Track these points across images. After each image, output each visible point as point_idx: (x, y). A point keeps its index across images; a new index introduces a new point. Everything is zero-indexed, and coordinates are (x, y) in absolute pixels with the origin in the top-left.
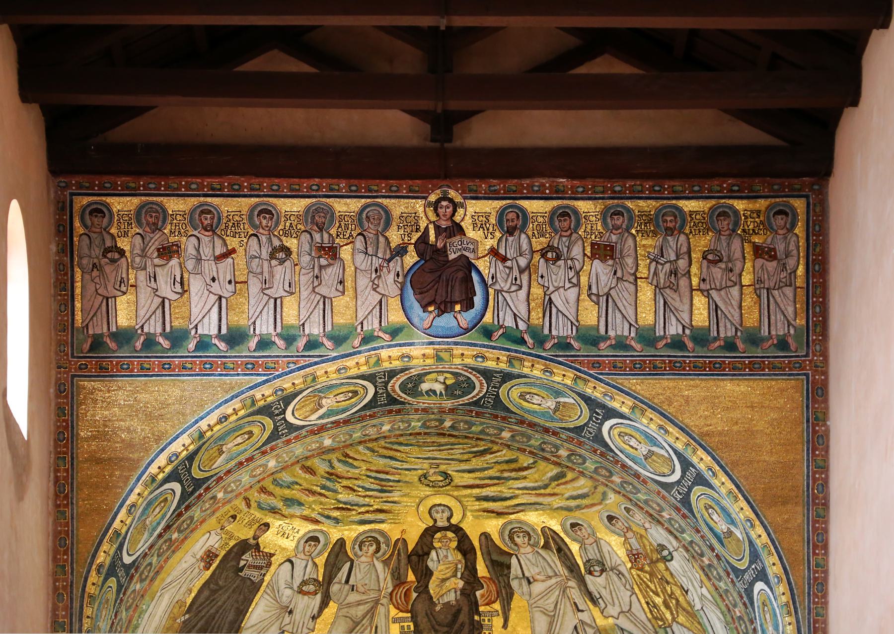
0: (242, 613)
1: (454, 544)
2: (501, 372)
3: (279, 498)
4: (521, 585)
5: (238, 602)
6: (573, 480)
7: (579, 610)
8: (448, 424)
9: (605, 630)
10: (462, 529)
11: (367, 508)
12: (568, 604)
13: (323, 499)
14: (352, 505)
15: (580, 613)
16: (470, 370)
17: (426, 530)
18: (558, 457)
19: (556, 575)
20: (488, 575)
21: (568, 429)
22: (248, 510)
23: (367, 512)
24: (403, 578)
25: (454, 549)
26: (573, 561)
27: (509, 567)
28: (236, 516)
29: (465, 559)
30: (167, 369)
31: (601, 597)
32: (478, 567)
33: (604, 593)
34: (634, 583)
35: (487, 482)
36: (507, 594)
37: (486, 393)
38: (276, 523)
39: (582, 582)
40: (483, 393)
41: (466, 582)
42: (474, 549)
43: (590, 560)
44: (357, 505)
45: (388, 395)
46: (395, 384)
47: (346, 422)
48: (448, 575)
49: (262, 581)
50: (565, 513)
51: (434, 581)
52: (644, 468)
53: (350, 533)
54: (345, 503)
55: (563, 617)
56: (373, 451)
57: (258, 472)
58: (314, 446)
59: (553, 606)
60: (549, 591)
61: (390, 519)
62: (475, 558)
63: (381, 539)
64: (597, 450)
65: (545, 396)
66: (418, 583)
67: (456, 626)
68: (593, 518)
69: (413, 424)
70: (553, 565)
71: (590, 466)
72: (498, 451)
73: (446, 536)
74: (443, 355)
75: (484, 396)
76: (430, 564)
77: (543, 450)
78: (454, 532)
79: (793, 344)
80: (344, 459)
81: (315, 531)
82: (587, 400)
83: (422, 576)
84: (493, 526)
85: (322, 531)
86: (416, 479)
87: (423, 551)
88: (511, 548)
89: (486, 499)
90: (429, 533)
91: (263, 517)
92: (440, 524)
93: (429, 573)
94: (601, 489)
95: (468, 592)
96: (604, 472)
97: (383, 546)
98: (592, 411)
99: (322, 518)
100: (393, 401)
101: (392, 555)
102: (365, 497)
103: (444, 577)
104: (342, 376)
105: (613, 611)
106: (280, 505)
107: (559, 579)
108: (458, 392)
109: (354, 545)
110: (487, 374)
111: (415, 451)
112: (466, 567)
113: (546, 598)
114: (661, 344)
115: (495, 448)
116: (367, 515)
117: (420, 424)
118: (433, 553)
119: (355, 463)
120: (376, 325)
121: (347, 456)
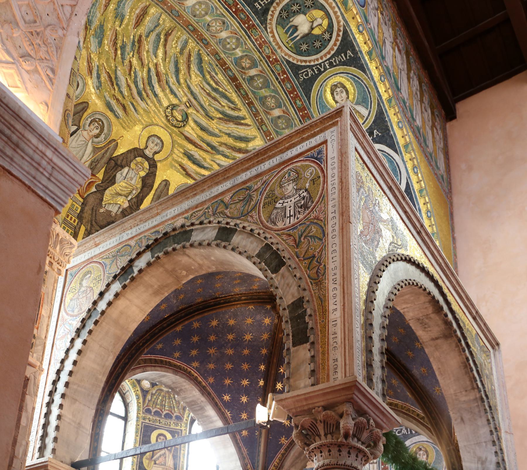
1: (143, 174)
8: (253, 72)
10: (156, 167)
25: (140, 177)
35: (204, 146)
37: (317, 65)
40: (316, 63)
66: (102, 183)
69: (237, 51)
75: (311, 67)
76: (118, 175)
78: (149, 166)
83: (107, 180)
87: (121, 163)
89: (190, 157)
117: (240, 54)
118: (126, 170)
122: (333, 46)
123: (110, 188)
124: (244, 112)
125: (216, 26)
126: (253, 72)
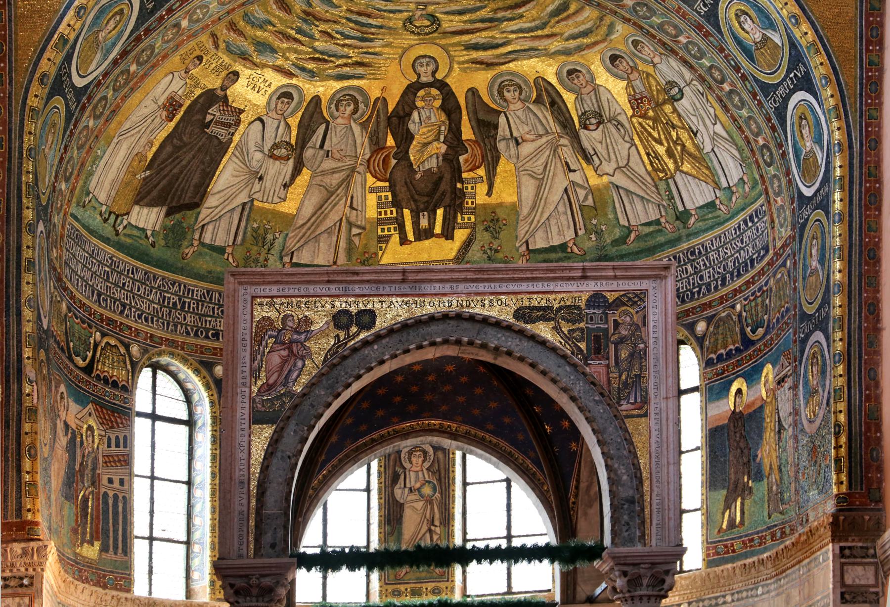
0: (208, 175)
1: (438, 103)
3: (250, 40)
4: (508, 147)
5: (203, 163)
7: (571, 171)
9: (599, 190)
11: (345, 61)
12: (559, 165)
14: (330, 56)
15: (571, 174)
17: (409, 87)
19: (547, 133)
20: (473, 137)
22: (215, 51)
23: (346, 65)
24: (381, 143)
25: (438, 109)
26: (567, 115)
27: (496, 127)
28: (202, 57)
29: (449, 120)
31: (596, 153)
32: (463, 129)
33: (599, 147)
34: (634, 132)
36: (492, 158)
38: (246, 73)
39: (575, 138)
41: (449, 147)
43: (586, 112)
44: (334, 56)
48: (430, 139)
51: (415, 146)
53: (326, 89)
54: (322, 53)
55: (552, 179)
59: (541, 168)
60: (539, 151)
61: (370, 74)
62: (461, 118)
63: (358, 97)
67: (438, 194)
70: (544, 121)
73: (429, 94)
76: (411, 127)
81: (288, 85)
85: (296, 87)
88: (499, 104)
91: (233, 63)
92: (424, 79)
93: (410, 137)
95: (450, 157)
97: (362, 106)
99: (297, 70)
101: (370, 117)
103: (426, 141)
105: (608, 167)
106: (251, 49)
107: (550, 138)
109: (330, 104)
112: (450, 130)
113: (535, 159)
116: (345, 68)
118: (415, 114)
123: (412, 147)
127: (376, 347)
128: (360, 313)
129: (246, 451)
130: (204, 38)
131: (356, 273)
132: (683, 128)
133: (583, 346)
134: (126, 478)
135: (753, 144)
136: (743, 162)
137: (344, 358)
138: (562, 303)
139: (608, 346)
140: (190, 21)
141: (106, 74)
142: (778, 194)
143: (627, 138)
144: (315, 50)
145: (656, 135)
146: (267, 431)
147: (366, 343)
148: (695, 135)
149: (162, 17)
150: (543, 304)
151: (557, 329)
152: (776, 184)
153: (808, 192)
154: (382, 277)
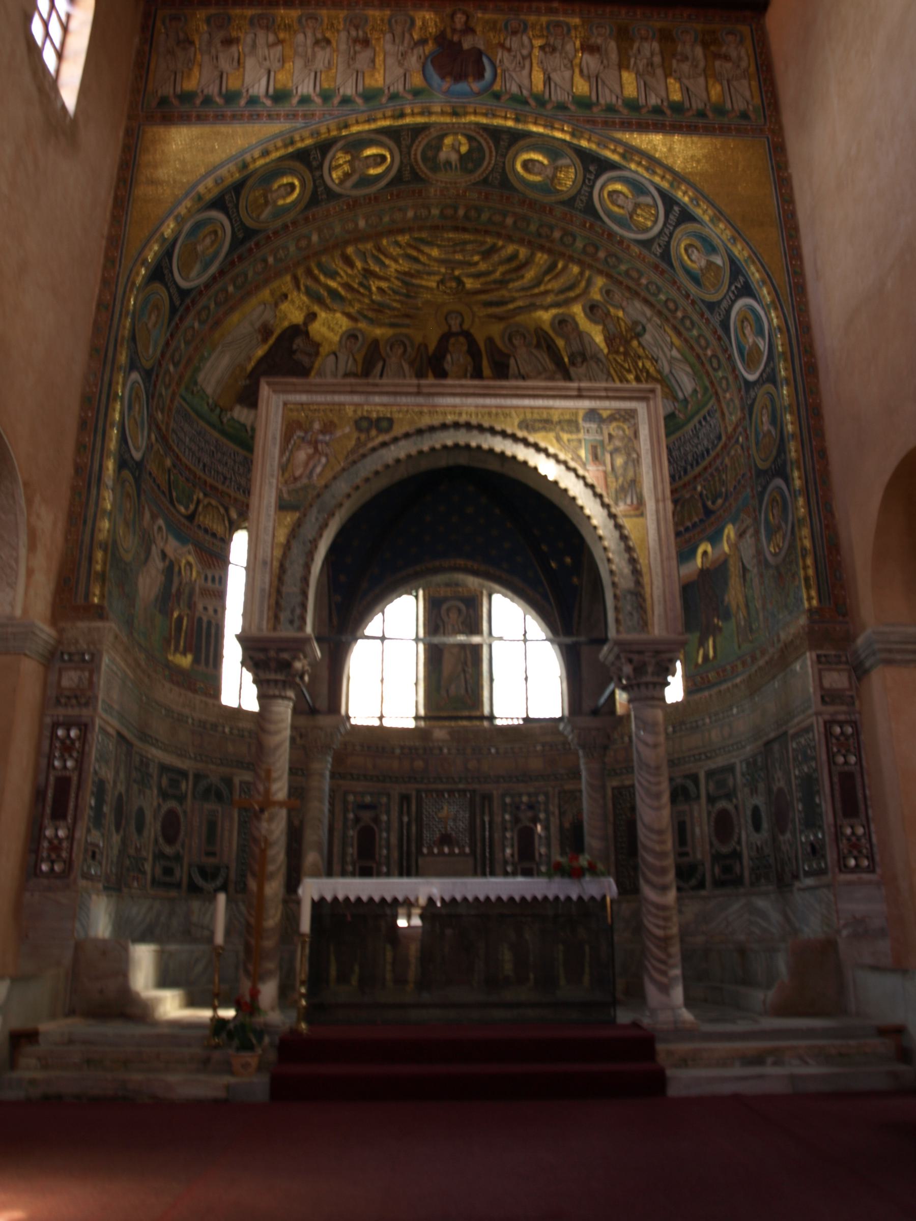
1: (465, 348)
2: (509, 130)
6: (565, 268)
8: (461, 212)
13: (358, 297)
16: (481, 132)
18: (552, 241)
21: (563, 203)
23: (396, 316)
27: (508, 367)
30: (220, 118)
35: (493, 286)
38: (323, 315)
42: (479, 351)
45: (412, 167)
46: (418, 149)
47: (376, 198)
49: (312, 368)
50: (554, 311)
52: (629, 229)
54: (379, 304)
56: (400, 246)
57: (303, 243)
58: (351, 226)
64: (585, 223)
65: (546, 162)
68: (577, 310)
71: (579, 244)
72: (503, 247)
74: (460, 110)
77: (540, 235)
79: (752, 116)
80: (376, 253)
82: (581, 153)
84: (496, 330)
85: (360, 330)
86: (434, 285)
90: (445, 338)
94: (587, 273)
96: (590, 250)
97: (409, 349)
98: (586, 170)
100: (416, 177)
102: (395, 300)
104: (373, 126)
108: (470, 166)
110: (495, 133)
111: (435, 252)
114: (644, 111)
115: (500, 243)
118: (449, 357)
119: (387, 262)
120: (401, 88)
121: (379, 249)
122: (486, 143)
124: (489, 240)
125: (398, 216)
126: (461, 212)
127: (392, 447)
128: (379, 420)
129: (271, 533)
130: (288, 278)
131: (376, 385)
132: (647, 357)
133: (583, 453)
134: (219, 609)
135: (703, 358)
136: (696, 375)
137: (364, 456)
138: (562, 417)
139: (603, 454)
140: (275, 259)
141: (207, 286)
142: (725, 391)
143: (605, 370)
144: (372, 301)
145: (626, 366)
146: (290, 518)
147: (384, 445)
148: (657, 361)
149: (250, 250)
150: (545, 416)
151: (558, 439)
152: (724, 383)
153: (751, 377)
154: (399, 389)
